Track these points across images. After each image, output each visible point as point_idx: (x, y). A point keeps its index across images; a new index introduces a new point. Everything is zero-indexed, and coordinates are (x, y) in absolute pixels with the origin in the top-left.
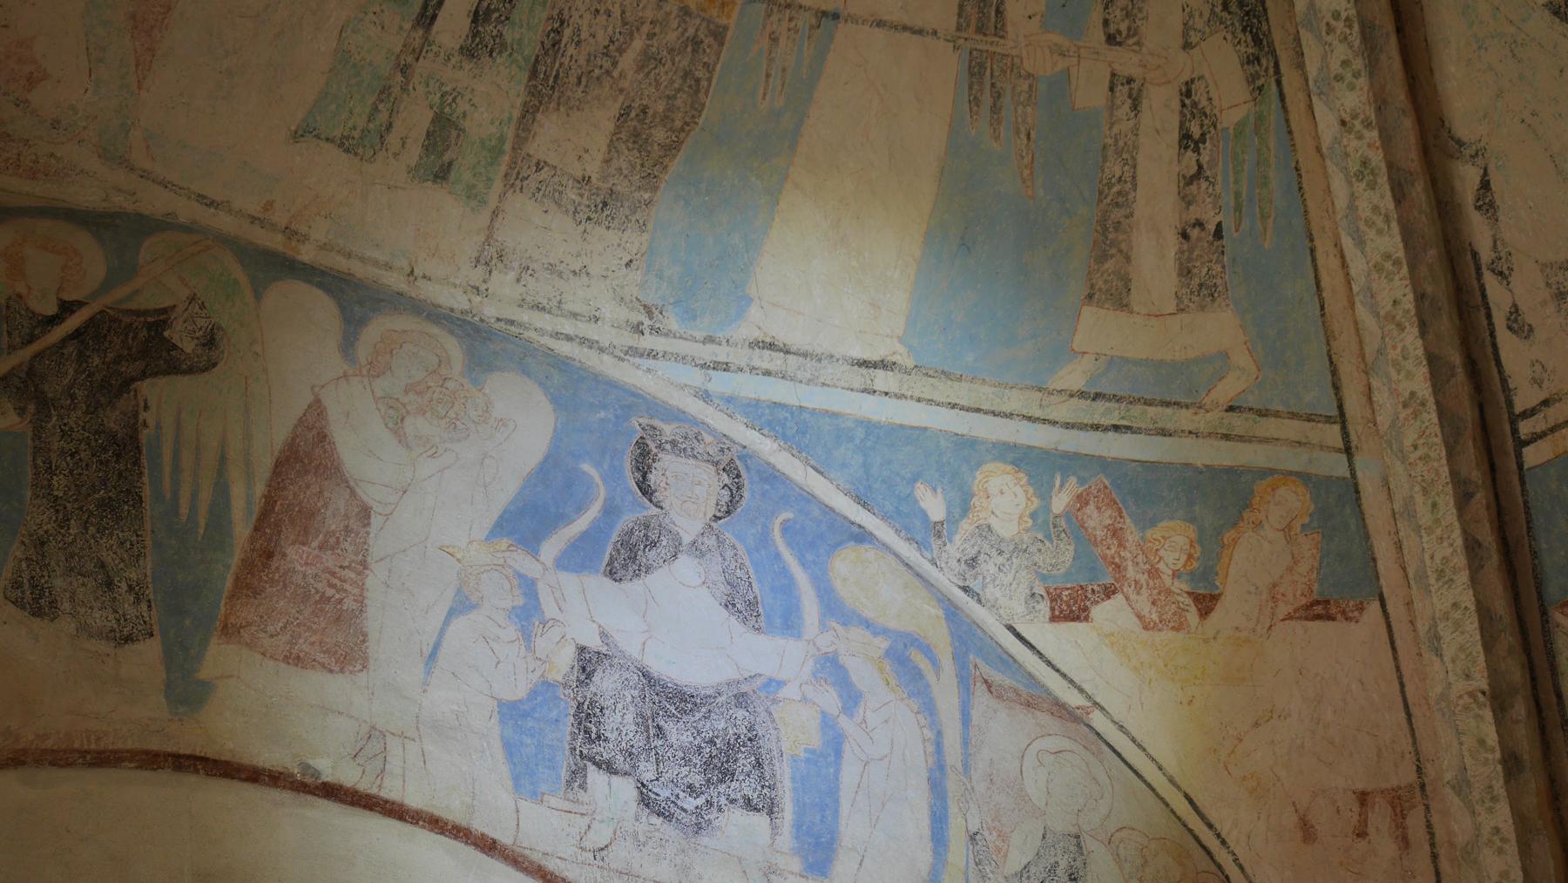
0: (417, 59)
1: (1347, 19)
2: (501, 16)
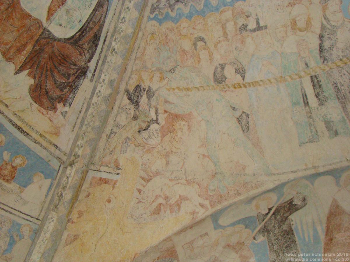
0: (311, 113)
2: (321, 92)
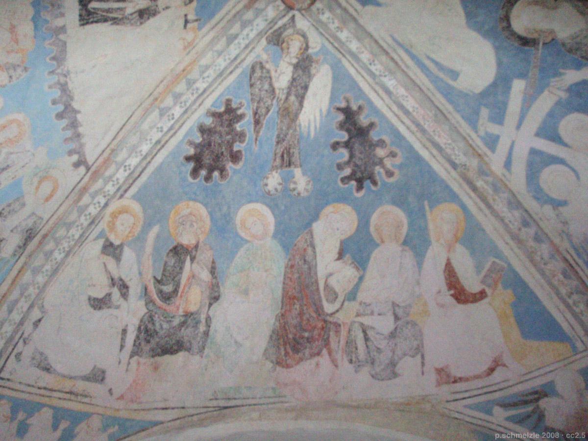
1: (57, 262)
